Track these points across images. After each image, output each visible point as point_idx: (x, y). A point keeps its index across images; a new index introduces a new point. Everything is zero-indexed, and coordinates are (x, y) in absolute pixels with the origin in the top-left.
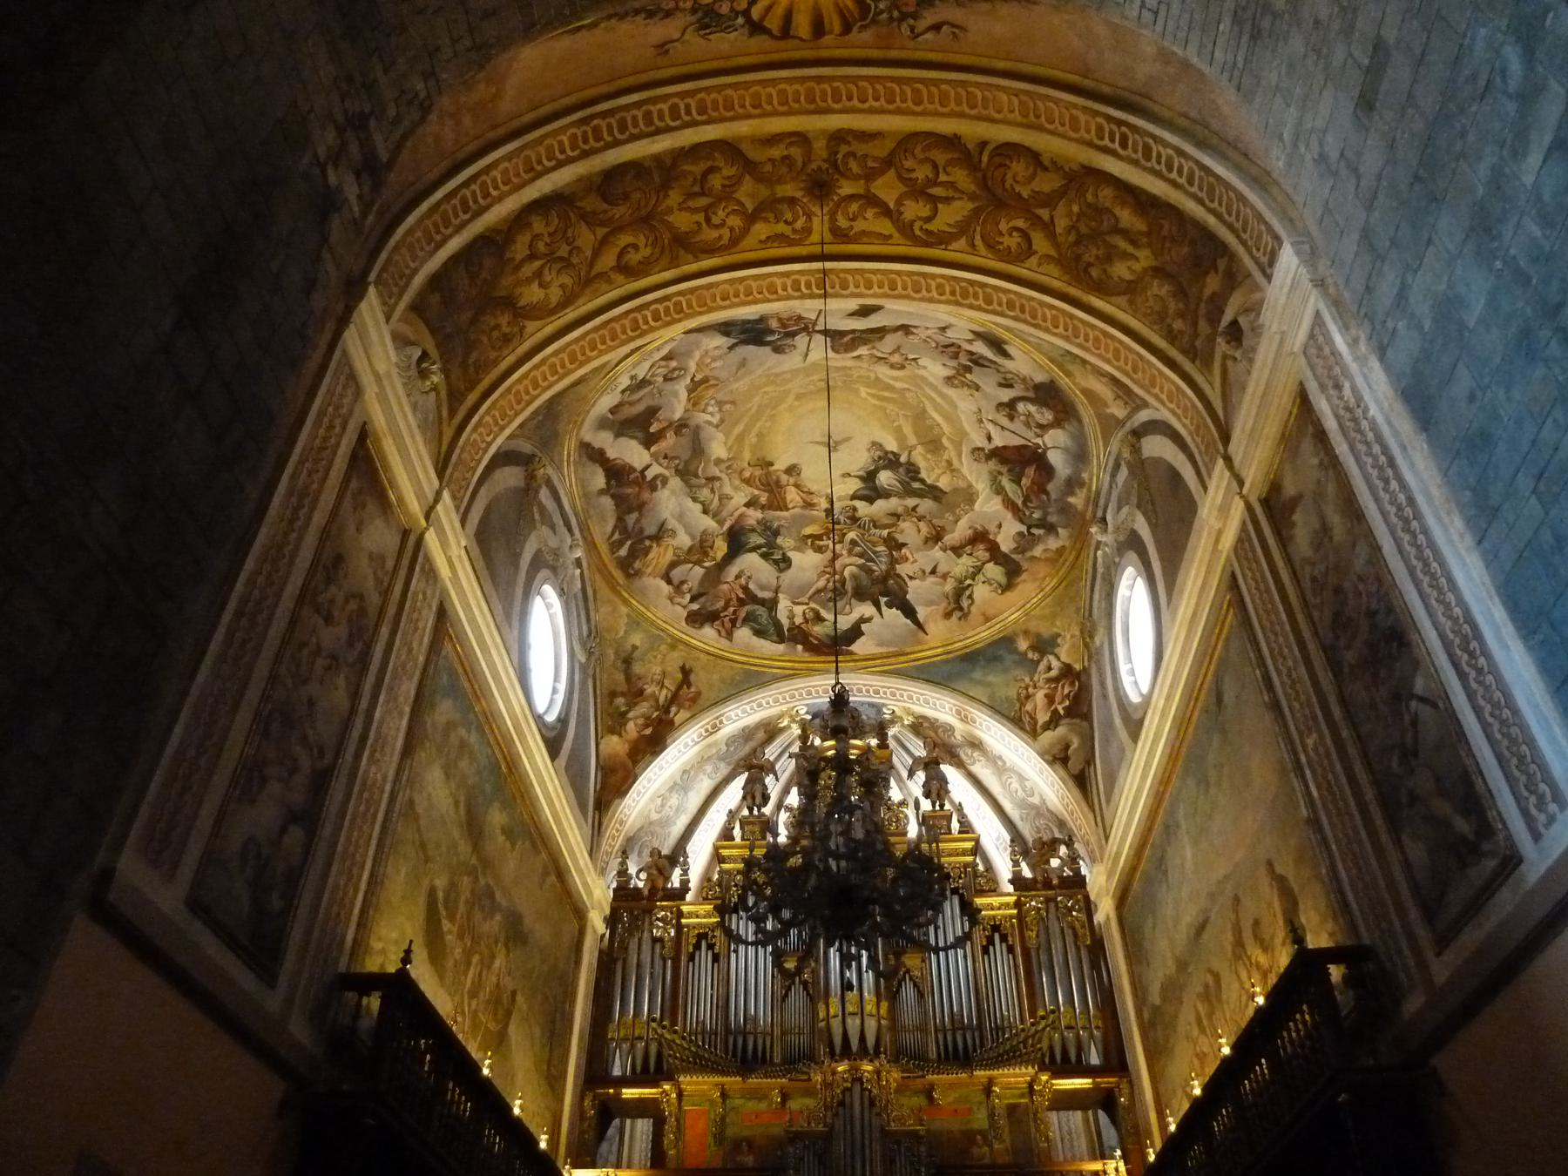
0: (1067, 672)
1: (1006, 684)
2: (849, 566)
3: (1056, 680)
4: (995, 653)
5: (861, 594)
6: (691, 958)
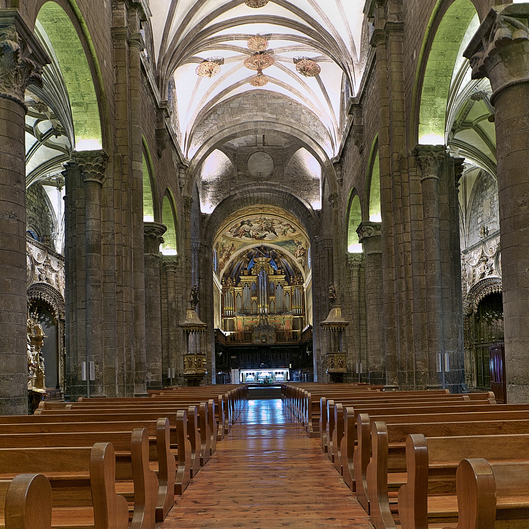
0: (303, 248)
1: (293, 248)
2: (264, 226)
3: (301, 249)
4: (290, 242)
5: (266, 230)
6: (237, 297)
